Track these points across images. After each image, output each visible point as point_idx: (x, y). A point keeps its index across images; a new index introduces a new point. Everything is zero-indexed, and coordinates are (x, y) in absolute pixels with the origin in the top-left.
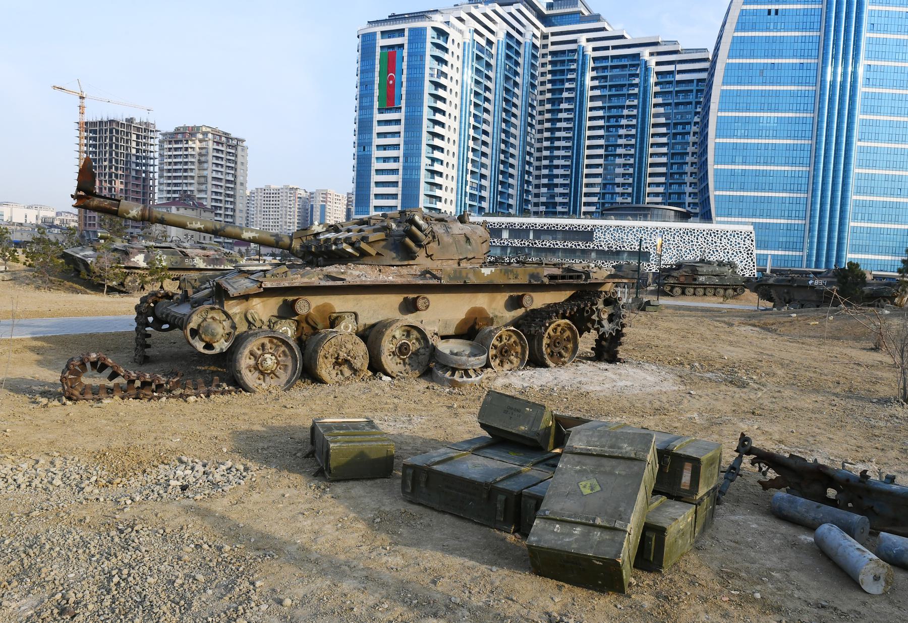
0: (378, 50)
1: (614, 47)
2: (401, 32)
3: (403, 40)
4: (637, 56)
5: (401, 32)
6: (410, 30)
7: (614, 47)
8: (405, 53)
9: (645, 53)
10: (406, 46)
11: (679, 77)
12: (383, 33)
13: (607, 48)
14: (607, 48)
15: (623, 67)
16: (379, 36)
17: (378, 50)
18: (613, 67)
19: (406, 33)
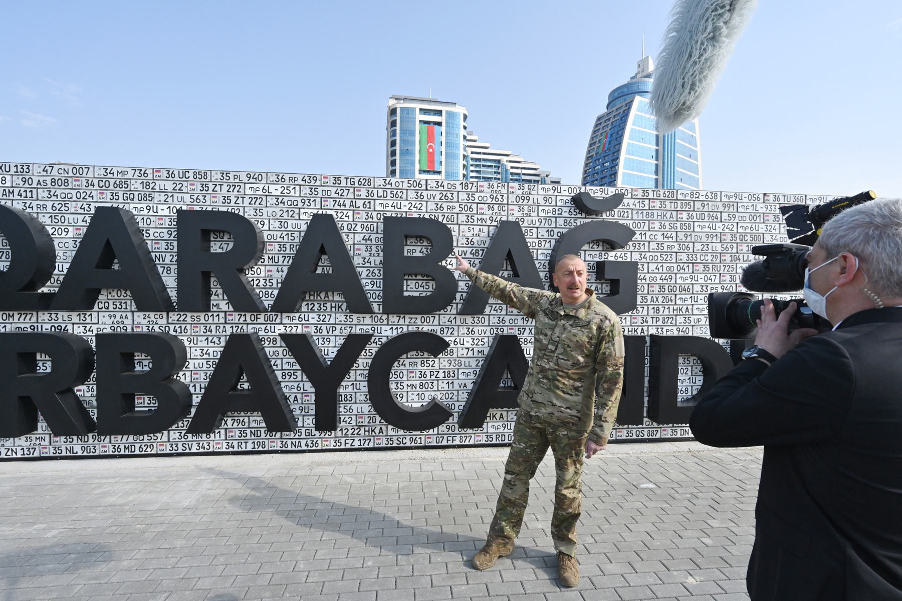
0: (417, 122)
1: (484, 154)
2: (439, 113)
3: (441, 119)
4: (499, 161)
5: (439, 113)
6: (447, 112)
7: (484, 154)
8: (443, 128)
9: (504, 159)
10: (444, 124)
11: (524, 177)
12: (421, 110)
13: (480, 153)
14: (480, 153)
15: (489, 166)
16: (418, 111)
17: (417, 122)
18: (484, 166)
19: (444, 113)
